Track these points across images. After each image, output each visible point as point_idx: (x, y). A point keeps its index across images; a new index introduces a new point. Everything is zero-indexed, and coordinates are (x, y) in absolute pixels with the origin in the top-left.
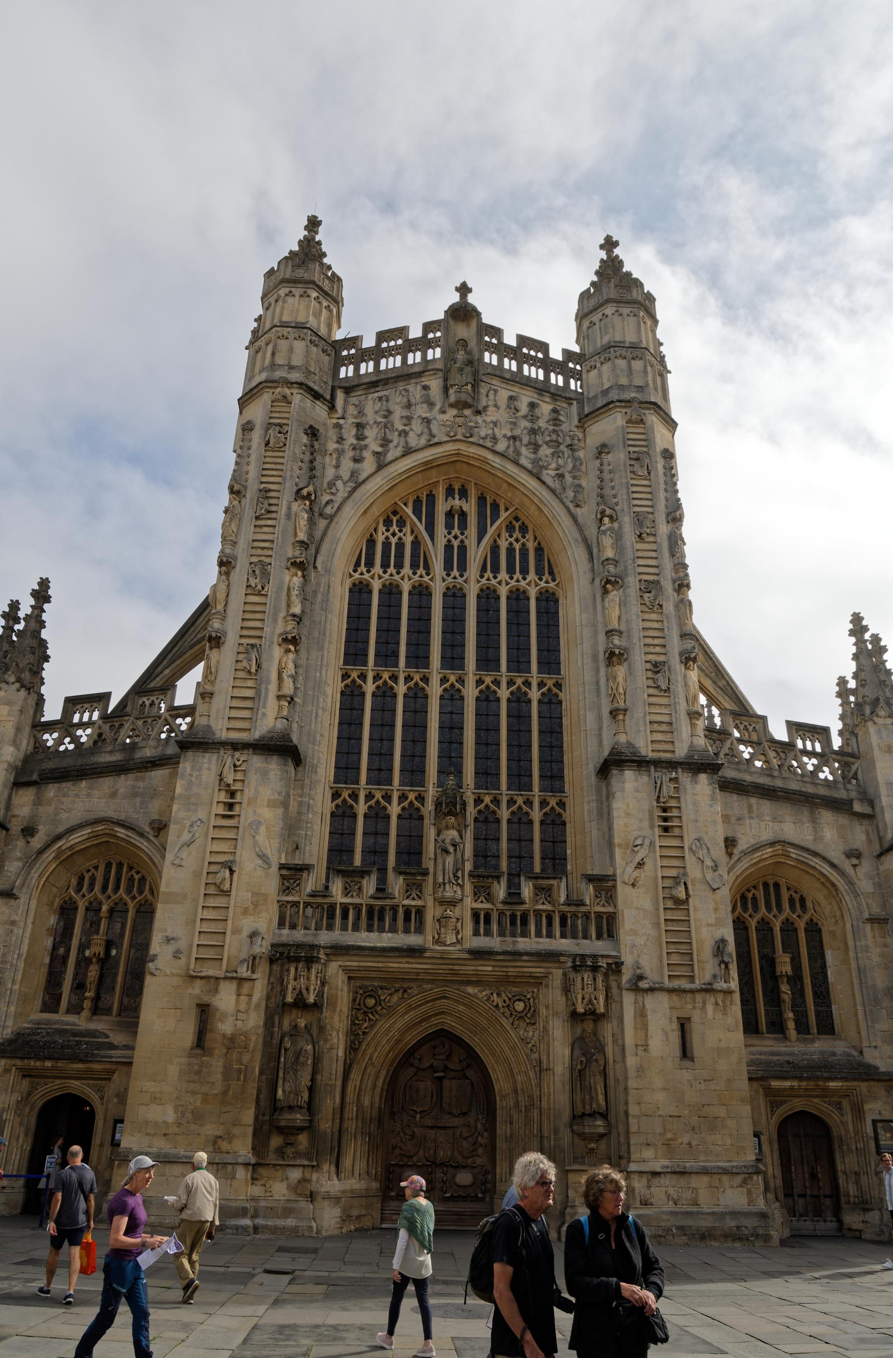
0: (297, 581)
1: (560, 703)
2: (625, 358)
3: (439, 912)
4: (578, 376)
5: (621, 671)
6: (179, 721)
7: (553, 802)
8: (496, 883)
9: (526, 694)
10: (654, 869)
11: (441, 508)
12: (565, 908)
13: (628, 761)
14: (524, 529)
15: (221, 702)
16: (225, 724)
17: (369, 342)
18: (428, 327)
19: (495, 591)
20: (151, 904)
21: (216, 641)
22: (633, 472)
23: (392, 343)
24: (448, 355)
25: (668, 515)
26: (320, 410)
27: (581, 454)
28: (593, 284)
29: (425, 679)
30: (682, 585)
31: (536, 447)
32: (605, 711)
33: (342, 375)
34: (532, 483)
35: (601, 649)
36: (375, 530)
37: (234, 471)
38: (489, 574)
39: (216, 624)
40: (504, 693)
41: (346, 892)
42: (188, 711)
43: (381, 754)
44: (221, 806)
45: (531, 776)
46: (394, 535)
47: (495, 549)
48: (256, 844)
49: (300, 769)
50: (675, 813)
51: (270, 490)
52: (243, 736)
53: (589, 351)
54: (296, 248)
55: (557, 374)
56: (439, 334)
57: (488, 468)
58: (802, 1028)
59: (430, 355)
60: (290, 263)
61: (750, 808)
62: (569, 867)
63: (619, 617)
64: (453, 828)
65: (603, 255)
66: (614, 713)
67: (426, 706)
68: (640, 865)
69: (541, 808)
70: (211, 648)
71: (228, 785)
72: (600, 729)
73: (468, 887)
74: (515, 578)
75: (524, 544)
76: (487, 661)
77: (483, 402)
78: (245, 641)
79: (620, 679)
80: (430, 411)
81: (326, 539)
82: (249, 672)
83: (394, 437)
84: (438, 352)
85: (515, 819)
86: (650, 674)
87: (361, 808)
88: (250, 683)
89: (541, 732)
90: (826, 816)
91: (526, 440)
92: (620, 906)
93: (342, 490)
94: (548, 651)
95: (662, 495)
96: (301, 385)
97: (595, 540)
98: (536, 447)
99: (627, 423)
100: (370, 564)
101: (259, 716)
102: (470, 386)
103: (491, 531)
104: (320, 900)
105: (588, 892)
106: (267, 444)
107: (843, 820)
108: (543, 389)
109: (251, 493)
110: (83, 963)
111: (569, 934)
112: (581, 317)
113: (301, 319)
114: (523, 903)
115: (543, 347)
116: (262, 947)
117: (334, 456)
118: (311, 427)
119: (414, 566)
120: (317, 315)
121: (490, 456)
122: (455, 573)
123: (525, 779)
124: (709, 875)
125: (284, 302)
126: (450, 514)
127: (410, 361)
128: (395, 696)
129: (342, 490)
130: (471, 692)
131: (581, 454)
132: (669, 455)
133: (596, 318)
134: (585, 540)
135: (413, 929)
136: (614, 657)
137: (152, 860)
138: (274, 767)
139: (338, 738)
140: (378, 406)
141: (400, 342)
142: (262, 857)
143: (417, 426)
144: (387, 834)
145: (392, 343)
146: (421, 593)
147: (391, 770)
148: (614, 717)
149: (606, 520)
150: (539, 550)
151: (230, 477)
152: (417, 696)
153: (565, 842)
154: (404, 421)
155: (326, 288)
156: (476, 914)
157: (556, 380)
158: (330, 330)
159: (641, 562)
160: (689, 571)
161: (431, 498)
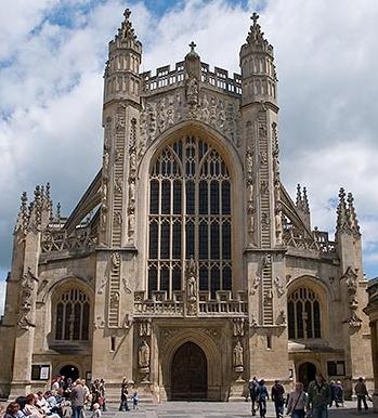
11: (185, 146)
14: (217, 154)
17: (153, 74)
18: (178, 65)
40: (209, 223)
47: (206, 163)
58: (309, 336)
66: (249, 232)
76: (203, 211)
90: (324, 265)
107: (330, 267)
110: (68, 323)
115: (226, 72)
116: (130, 319)
119: (175, 173)
126: (188, 149)
130: (197, 223)
146: (178, 184)
150: (223, 163)
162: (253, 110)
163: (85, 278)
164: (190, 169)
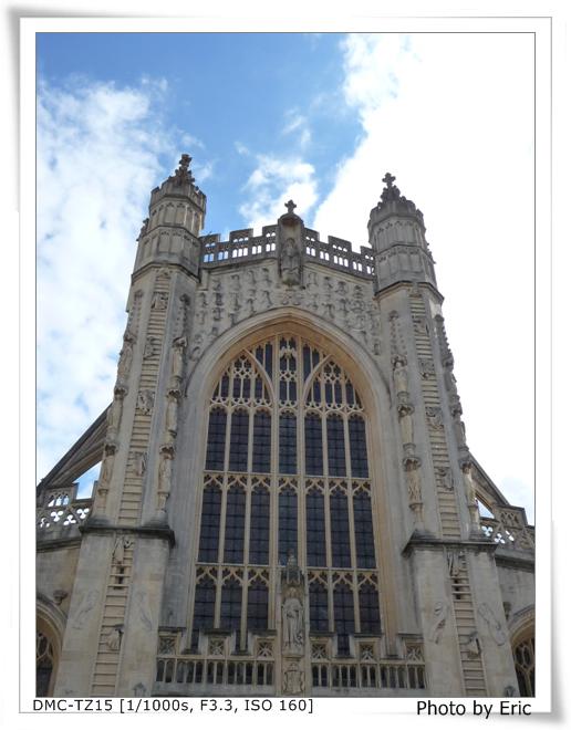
0: (174, 406)
1: (369, 499)
2: (405, 253)
3: (287, 665)
4: (372, 264)
5: (416, 474)
6: (79, 511)
7: (367, 576)
8: (330, 640)
9: (343, 492)
10: (450, 629)
11: (278, 354)
12: (385, 662)
13: (428, 543)
14: (337, 370)
15: (113, 496)
16: (116, 514)
17: (225, 238)
18: (266, 229)
19: (318, 415)
20: (50, 662)
21: (111, 450)
22: (416, 331)
23: (241, 240)
24: (281, 247)
25: (442, 361)
26: (192, 282)
27: (377, 318)
28: (379, 203)
29: (268, 481)
30: (457, 411)
31: (346, 312)
32: (406, 505)
33: (206, 260)
34: (343, 338)
35: (400, 458)
36: (229, 370)
37: (128, 325)
38: (313, 403)
39: (111, 436)
40: (327, 492)
41: (211, 650)
42: (88, 503)
43: (234, 539)
44: (113, 579)
45: (349, 555)
46: (242, 373)
47: (317, 385)
48: (142, 610)
49: (174, 550)
50: (464, 583)
51: (154, 339)
52: (132, 524)
53: (381, 247)
54: (174, 175)
55: (357, 263)
56: (274, 234)
57: (310, 326)
59: (268, 248)
60: (171, 185)
61: (518, 578)
62: (382, 628)
63: (413, 435)
64: (295, 597)
65: (385, 185)
66: (412, 507)
67: (268, 501)
68: (441, 625)
69: (359, 581)
70: (107, 455)
71: (120, 563)
72: (402, 518)
73: (308, 646)
74: (332, 405)
75: (337, 382)
76: (314, 466)
77: (306, 281)
78: (133, 450)
79: (416, 480)
80: (269, 286)
81: (194, 376)
82: (137, 474)
83: (242, 303)
84: (274, 246)
85: (339, 590)
86: (438, 477)
87: (220, 582)
88: (138, 482)
89: (356, 521)
91: (338, 307)
92: (428, 660)
93: (206, 340)
94: (359, 459)
95: (437, 347)
96: (179, 265)
97: (391, 379)
98: (346, 312)
99: (411, 296)
100: (225, 394)
101: (144, 508)
102: (297, 271)
103: (313, 371)
104: (192, 657)
105: (401, 648)
106: (153, 306)
108: (349, 271)
109: (141, 341)
111: (388, 684)
112: (372, 225)
113: (178, 222)
114: (352, 658)
115: (347, 244)
117: (201, 316)
118: (185, 296)
119: (258, 396)
120: (189, 219)
121: (313, 319)
122: (288, 401)
123: (345, 559)
124: (495, 633)
125: (166, 210)
126: (283, 359)
127: (254, 252)
128: (244, 493)
129: (206, 340)
130: (302, 491)
131: (377, 318)
132: (440, 319)
133: (383, 226)
134: (383, 379)
135: (265, 681)
136: (411, 464)
137: (53, 623)
138: (157, 547)
139: (202, 526)
140: (232, 282)
141: (247, 239)
142: (145, 620)
143: (259, 296)
144: (240, 603)
145: (241, 240)
146: (263, 416)
147: (242, 551)
148: (413, 509)
149: (399, 364)
150: (349, 386)
151: (124, 328)
152: (261, 494)
153: (378, 608)
154: (251, 293)
155: (196, 202)
156: (315, 670)
157: (358, 267)
158: (197, 226)
159: (426, 394)
160: (461, 400)
161: (270, 348)
162: (401, 294)
163: (51, 598)
164: (288, 391)
